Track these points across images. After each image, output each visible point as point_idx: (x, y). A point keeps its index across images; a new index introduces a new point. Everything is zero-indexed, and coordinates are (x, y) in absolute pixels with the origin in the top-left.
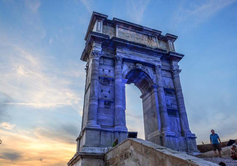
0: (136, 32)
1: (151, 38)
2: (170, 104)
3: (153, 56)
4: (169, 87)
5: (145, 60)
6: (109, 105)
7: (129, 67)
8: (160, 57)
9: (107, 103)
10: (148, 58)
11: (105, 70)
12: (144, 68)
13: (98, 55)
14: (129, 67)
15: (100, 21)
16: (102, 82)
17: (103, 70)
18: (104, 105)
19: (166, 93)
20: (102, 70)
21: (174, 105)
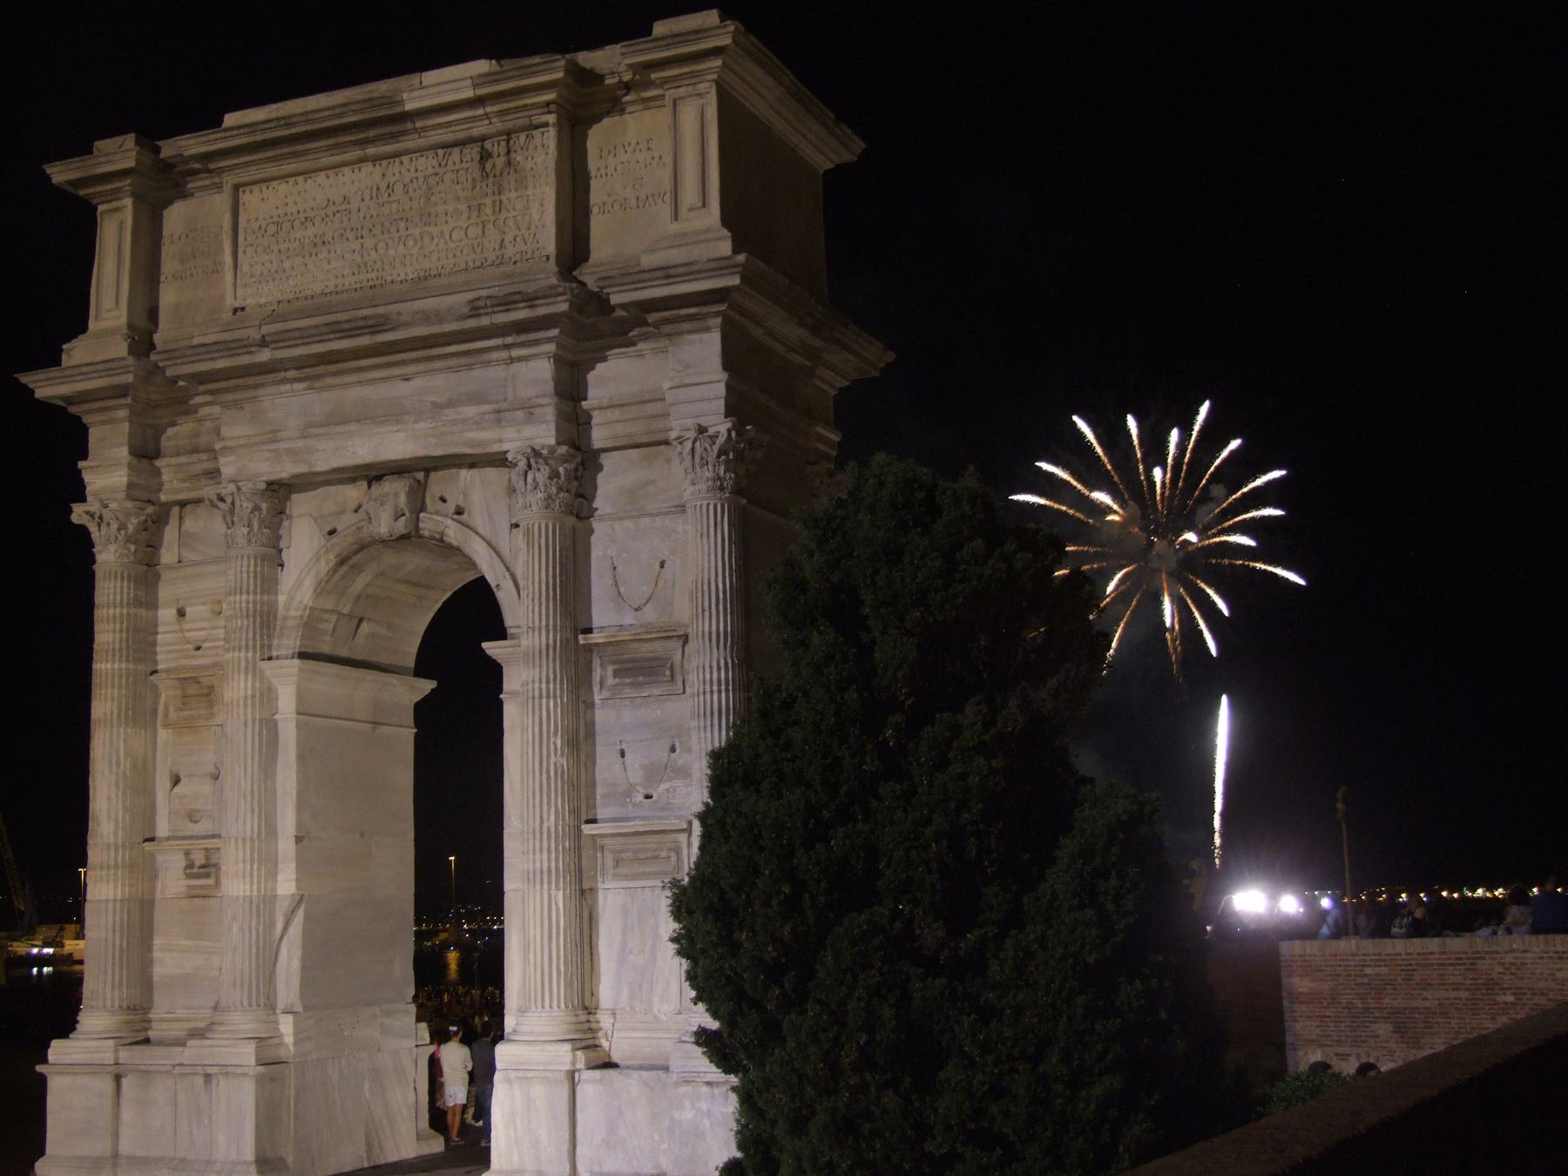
0: (376, 159)
1: (500, 162)
3: (487, 363)
4: (649, 614)
6: (208, 876)
7: (332, 532)
8: (551, 348)
9: (199, 859)
10: (451, 404)
11: (189, 610)
12: (444, 500)
13: (108, 524)
14: (332, 532)
15: (118, 210)
16: (173, 714)
17: (181, 613)
18: (189, 876)
19: (610, 681)
20: (174, 611)
21: (679, 783)
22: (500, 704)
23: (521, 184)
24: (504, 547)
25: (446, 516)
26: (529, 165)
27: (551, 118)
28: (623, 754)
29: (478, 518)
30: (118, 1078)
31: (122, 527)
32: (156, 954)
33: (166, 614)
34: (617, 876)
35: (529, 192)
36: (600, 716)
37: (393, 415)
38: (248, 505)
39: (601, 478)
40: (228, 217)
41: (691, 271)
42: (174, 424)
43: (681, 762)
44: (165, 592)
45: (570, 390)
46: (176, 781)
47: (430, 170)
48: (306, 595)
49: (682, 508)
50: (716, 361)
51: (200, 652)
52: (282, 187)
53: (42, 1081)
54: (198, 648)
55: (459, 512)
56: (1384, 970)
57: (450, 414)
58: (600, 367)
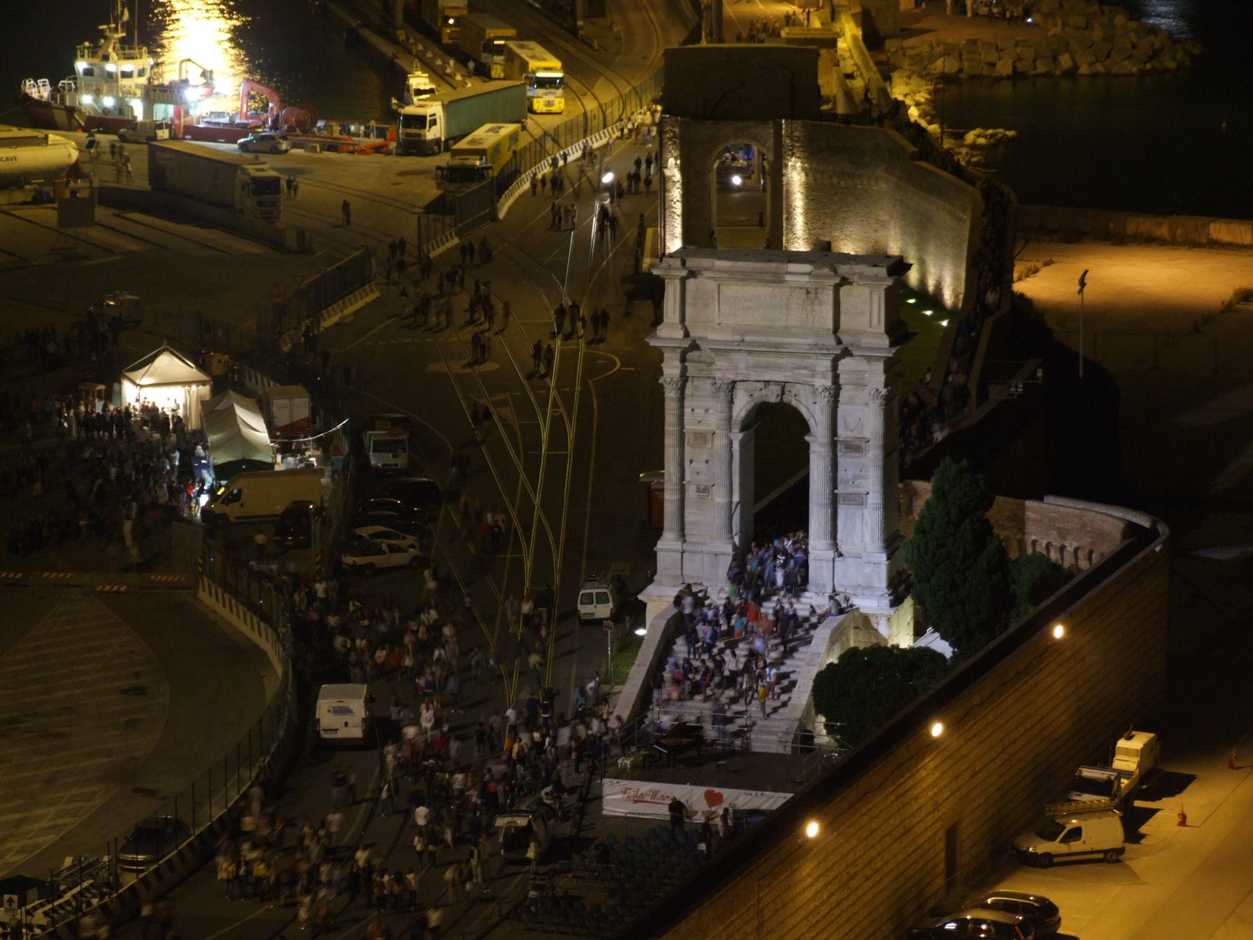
1: (813, 296)
2: (850, 477)
3: (809, 358)
4: (856, 434)
5: (785, 376)
9: (702, 487)
10: (797, 368)
11: (695, 410)
17: (693, 410)
20: (690, 410)
23: (820, 304)
24: (811, 410)
26: (823, 299)
29: (803, 399)
33: (687, 411)
34: (844, 504)
36: (841, 460)
37: (779, 368)
38: (725, 387)
39: (841, 392)
40: (716, 295)
41: (879, 349)
44: (687, 403)
45: (835, 367)
46: (691, 461)
48: (743, 414)
49: (867, 404)
50: (882, 370)
52: (736, 288)
53: (655, 553)
56: (1056, 515)
57: (798, 372)
58: (842, 360)
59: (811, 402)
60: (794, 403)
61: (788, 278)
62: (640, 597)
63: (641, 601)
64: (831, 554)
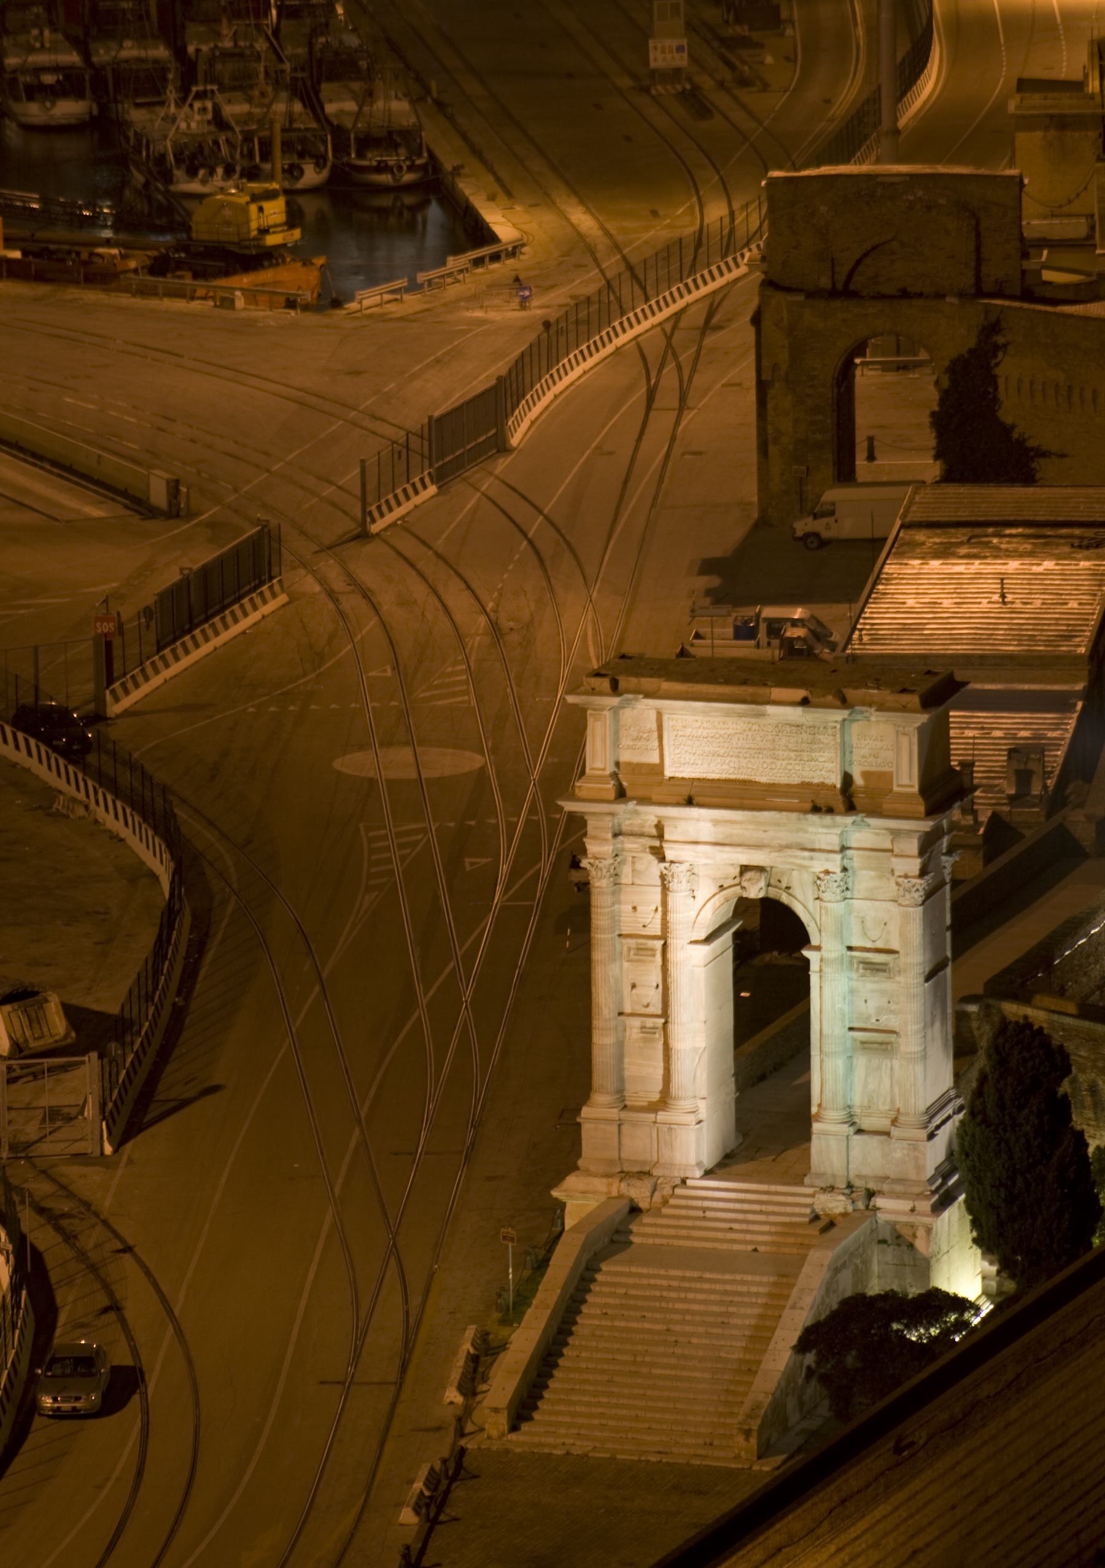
8: (839, 832)
10: (788, 847)
11: (639, 908)
12: (779, 881)
17: (635, 908)
18: (642, 1032)
19: (861, 971)
20: (630, 908)
22: (809, 976)
25: (781, 889)
27: (838, 726)
28: (866, 1001)
29: (797, 891)
30: (620, 1126)
31: (609, 871)
32: (625, 1066)
35: (826, 754)
42: (629, 819)
43: (893, 1008)
46: (634, 986)
47: (774, 733)
51: (646, 929)
54: (644, 926)
55: (788, 888)
57: (789, 852)
59: (811, 897)
60: (785, 899)
61: (770, 709)
62: (555, 1193)
63: (556, 1199)
64: (846, 1129)
